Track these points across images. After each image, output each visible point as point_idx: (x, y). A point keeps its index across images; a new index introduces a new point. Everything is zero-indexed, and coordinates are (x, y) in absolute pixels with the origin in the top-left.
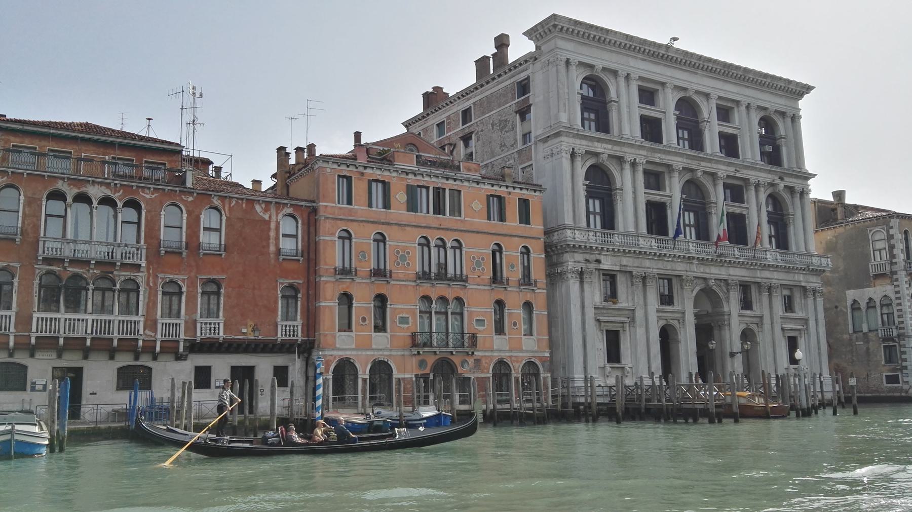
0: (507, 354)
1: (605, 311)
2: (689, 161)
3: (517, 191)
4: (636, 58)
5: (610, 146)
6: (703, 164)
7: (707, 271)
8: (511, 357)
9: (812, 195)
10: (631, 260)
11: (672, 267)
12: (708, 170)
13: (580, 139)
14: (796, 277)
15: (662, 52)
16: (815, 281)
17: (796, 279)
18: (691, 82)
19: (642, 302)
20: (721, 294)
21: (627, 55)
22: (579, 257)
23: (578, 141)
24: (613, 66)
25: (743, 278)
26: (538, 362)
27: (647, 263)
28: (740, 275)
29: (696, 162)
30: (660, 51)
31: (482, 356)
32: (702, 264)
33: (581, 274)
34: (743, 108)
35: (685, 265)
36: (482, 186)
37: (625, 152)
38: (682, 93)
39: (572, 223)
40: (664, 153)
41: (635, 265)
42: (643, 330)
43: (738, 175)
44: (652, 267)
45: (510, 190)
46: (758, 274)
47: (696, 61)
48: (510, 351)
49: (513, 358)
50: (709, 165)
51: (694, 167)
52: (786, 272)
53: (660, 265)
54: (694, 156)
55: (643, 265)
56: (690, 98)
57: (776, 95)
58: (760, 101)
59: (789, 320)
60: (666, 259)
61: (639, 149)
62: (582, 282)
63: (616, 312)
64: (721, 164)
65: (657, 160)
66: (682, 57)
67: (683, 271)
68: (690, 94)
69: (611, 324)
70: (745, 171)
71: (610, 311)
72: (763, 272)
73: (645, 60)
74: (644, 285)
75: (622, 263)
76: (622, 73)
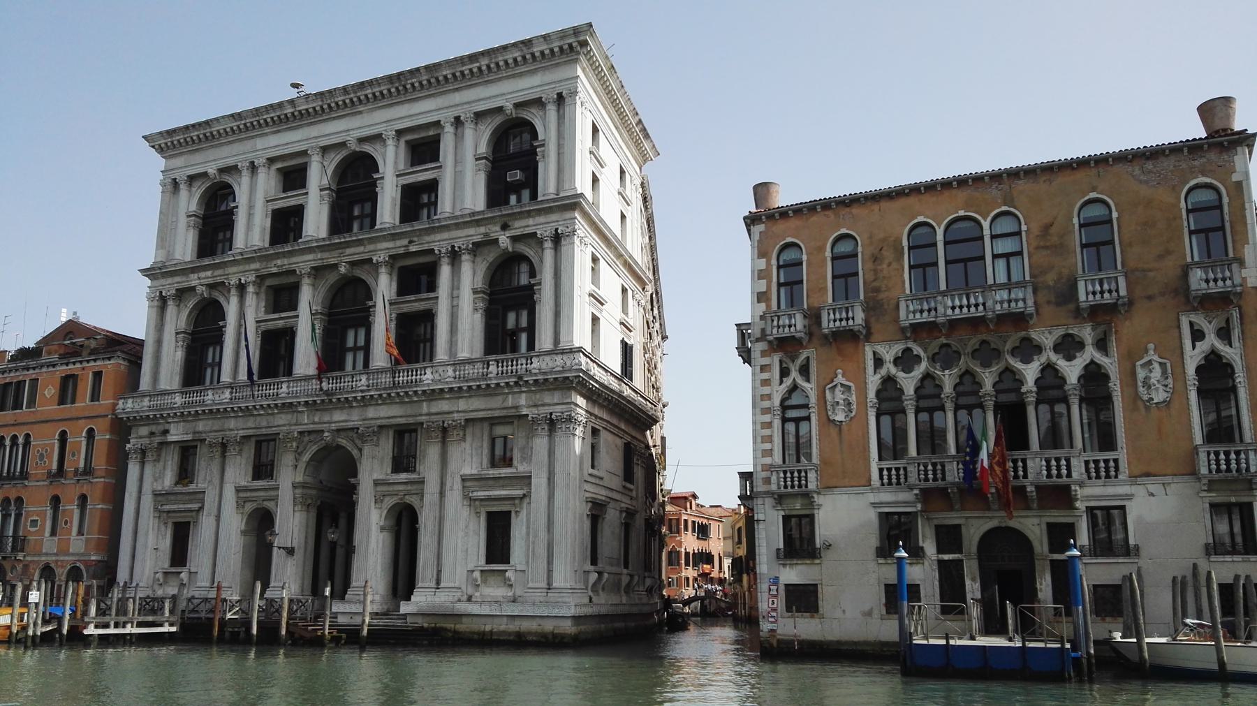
0: (54, 558)
1: (172, 498)
2: (326, 255)
3: (92, 364)
4: (266, 134)
5: (209, 273)
6: (348, 251)
7: (326, 418)
8: (57, 561)
9: (754, 210)
10: (210, 422)
11: (268, 423)
12: (356, 258)
13: (172, 276)
14: (510, 401)
15: (289, 110)
16: (555, 401)
17: (510, 405)
18: (348, 130)
19: (216, 481)
20: (355, 452)
21: (252, 137)
22: (144, 431)
23: (163, 281)
24: (230, 162)
25: (391, 420)
26: (82, 567)
27: (232, 424)
28: (386, 415)
29: (336, 253)
30: (285, 112)
31: (31, 561)
32: (317, 410)
33: (143, 452)
34: (449, 129)
35: (289, 416)
36: (58, 368)
37: (227, 275)
38: (343, 152)
39: (446, 358)
40: (284, 257)
41: (215, 428)
42: (212, 520)
43: (413, 248)
44: (236, 427)
45: (85, 364)
46: (425, 408)
47: (343, 98)
48: (56, 554)
49: (59, 563)
50: (361, 249)
51: (332, 261)
52: (485, 396)
53: (251, 423)
54: (340, 243)
55: (226, 426)
56: (355, 153)
57: (521, 75)
58: (482, 102)
59: (491, 482)
60: (255, 413)
61: (249, 263)
62: (143, 463)
63: (187, 498)
64: (380, 242)
65: (274, 270)
66: (320, 103)
67: (284, 425)
68: (354, 146)
69: (178, 514)
70: (427, 238)
71: (180, 497)
72: (434, 403)
73: (278, 131)
74: (223, 456)
75: (197, 429)
76: (243, 165)
